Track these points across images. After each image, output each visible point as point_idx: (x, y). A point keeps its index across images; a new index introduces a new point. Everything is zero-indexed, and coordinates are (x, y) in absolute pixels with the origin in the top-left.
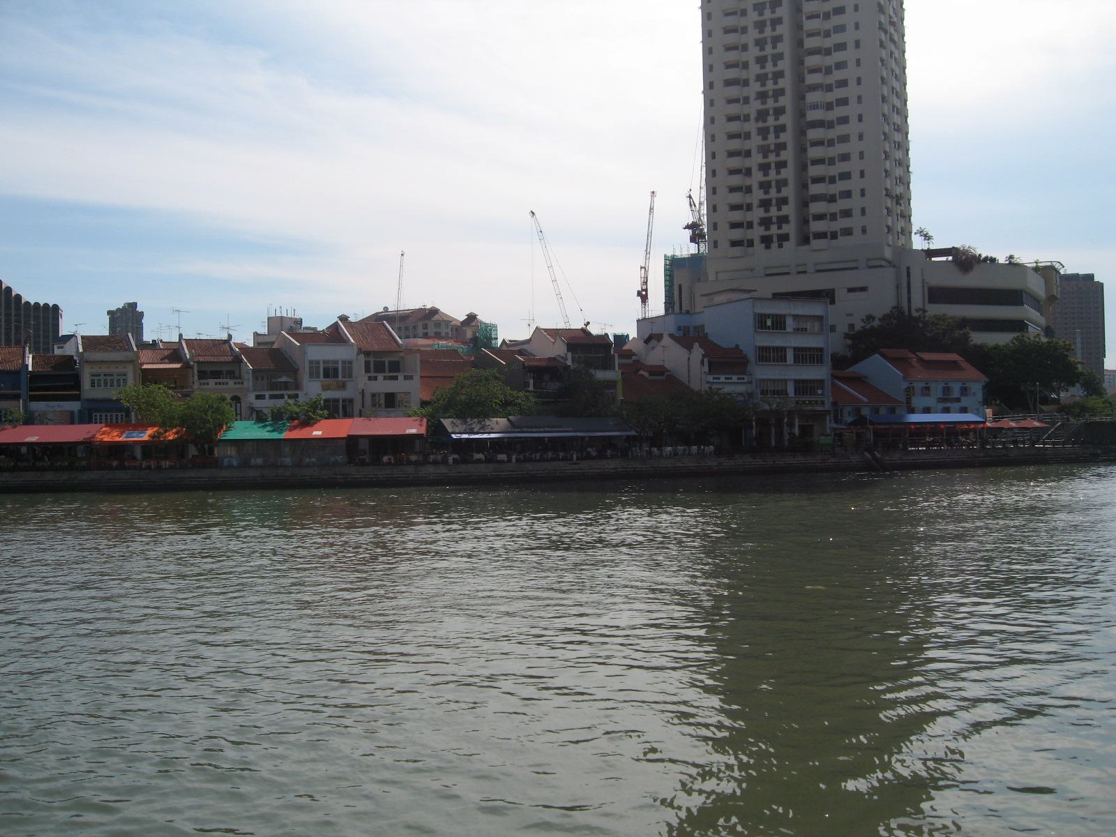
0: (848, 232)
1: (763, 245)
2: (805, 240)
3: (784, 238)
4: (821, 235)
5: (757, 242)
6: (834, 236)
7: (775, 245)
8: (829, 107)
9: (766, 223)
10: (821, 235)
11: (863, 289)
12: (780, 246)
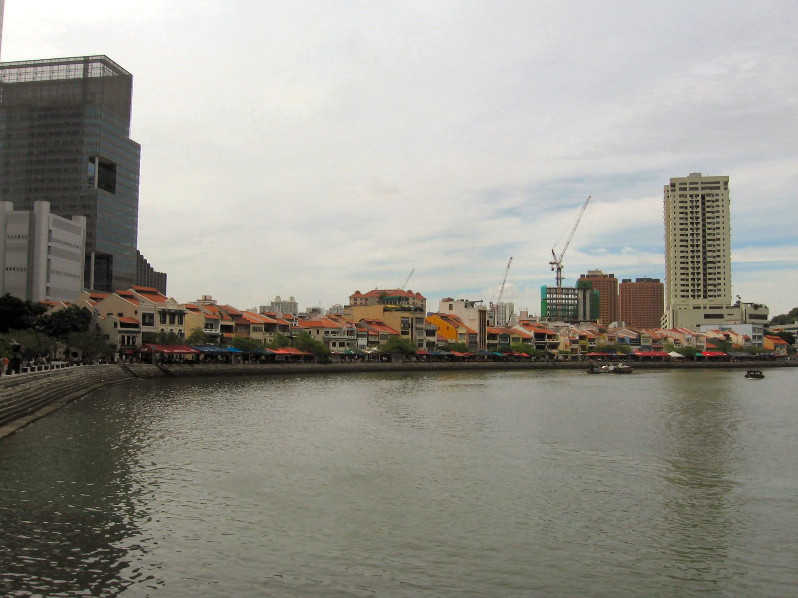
0: (719, 296)
1: (692, 298)
3: (699, 296)
4: (711, 296)
5: (690, 296)
6: (715, 296)
7: (696, 298)
8: (714, 257)
10: (711, 296)
11: (732, 315)
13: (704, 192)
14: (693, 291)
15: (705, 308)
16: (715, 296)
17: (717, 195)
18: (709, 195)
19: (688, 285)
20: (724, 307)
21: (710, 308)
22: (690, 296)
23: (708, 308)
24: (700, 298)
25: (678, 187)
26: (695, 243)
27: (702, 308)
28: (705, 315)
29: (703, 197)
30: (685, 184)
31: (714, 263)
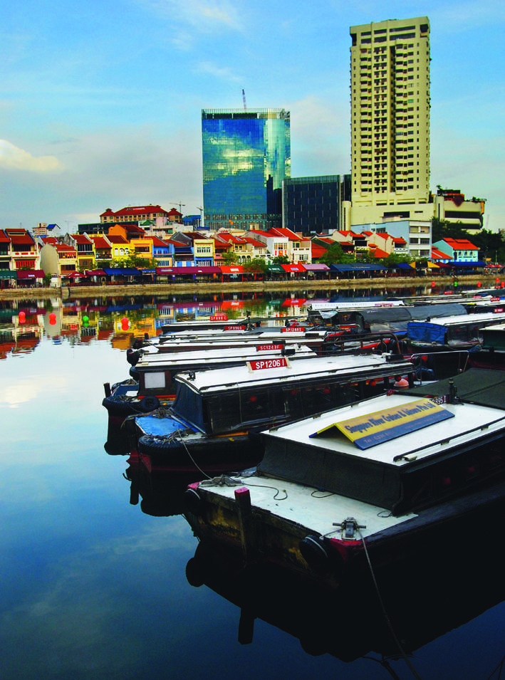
0: (411, 187)
3: (384, 189)
4: (400, 188)
5: (373, 190)
6: (405, 189)
7: (381, 191)
8: (405, 134)
9: (377, 182)
10: (400, 188)
12: (383, 192)
13: (392, 43)
15: (392, 204)
16: (405, 189)
17: (411, 46)
18: (400, 46)
19: (370, 175)
20: (417, 202)
21: (399, 204)
22: (373, 190)
23: (396, 203)
24: (385, 191)
25: (359, 38)
27: (388, 204)
28: (385, 213)
29: (392, 49)
30: (369, 33)
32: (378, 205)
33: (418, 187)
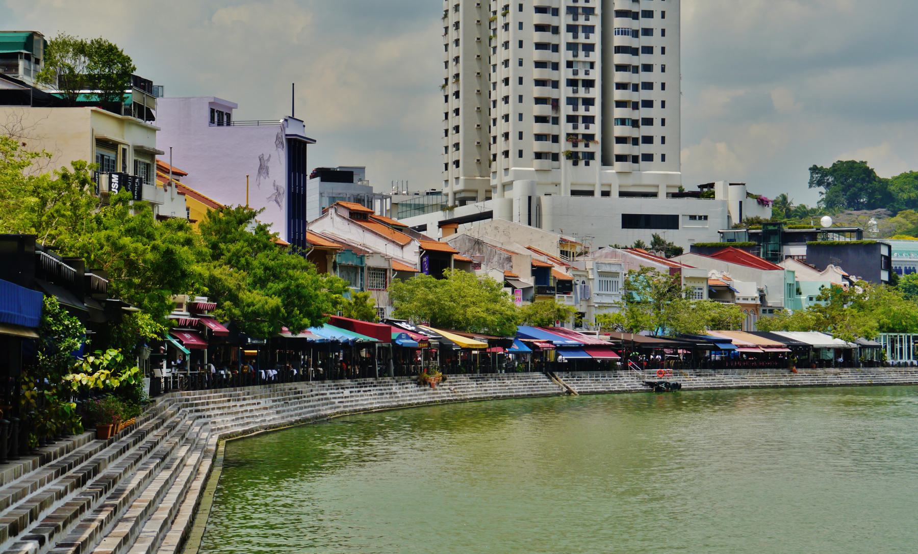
2: (606, 162)
3: (590, 156)
4: (620, 158)
6: (635, 159)
7: (582, 163)
10: (620, 158)
12: (587, 164)
14: (573, 138)
15: (606, 194)
16: (635, 159)
24: (591, 162)
26: (581, 111)
27: (597, 193)
31: (634, 52)
32: (574, 193)
33: (663, 158)
